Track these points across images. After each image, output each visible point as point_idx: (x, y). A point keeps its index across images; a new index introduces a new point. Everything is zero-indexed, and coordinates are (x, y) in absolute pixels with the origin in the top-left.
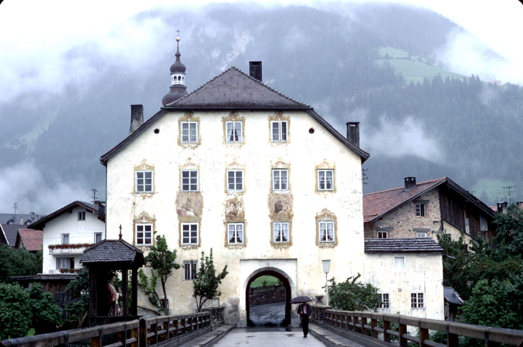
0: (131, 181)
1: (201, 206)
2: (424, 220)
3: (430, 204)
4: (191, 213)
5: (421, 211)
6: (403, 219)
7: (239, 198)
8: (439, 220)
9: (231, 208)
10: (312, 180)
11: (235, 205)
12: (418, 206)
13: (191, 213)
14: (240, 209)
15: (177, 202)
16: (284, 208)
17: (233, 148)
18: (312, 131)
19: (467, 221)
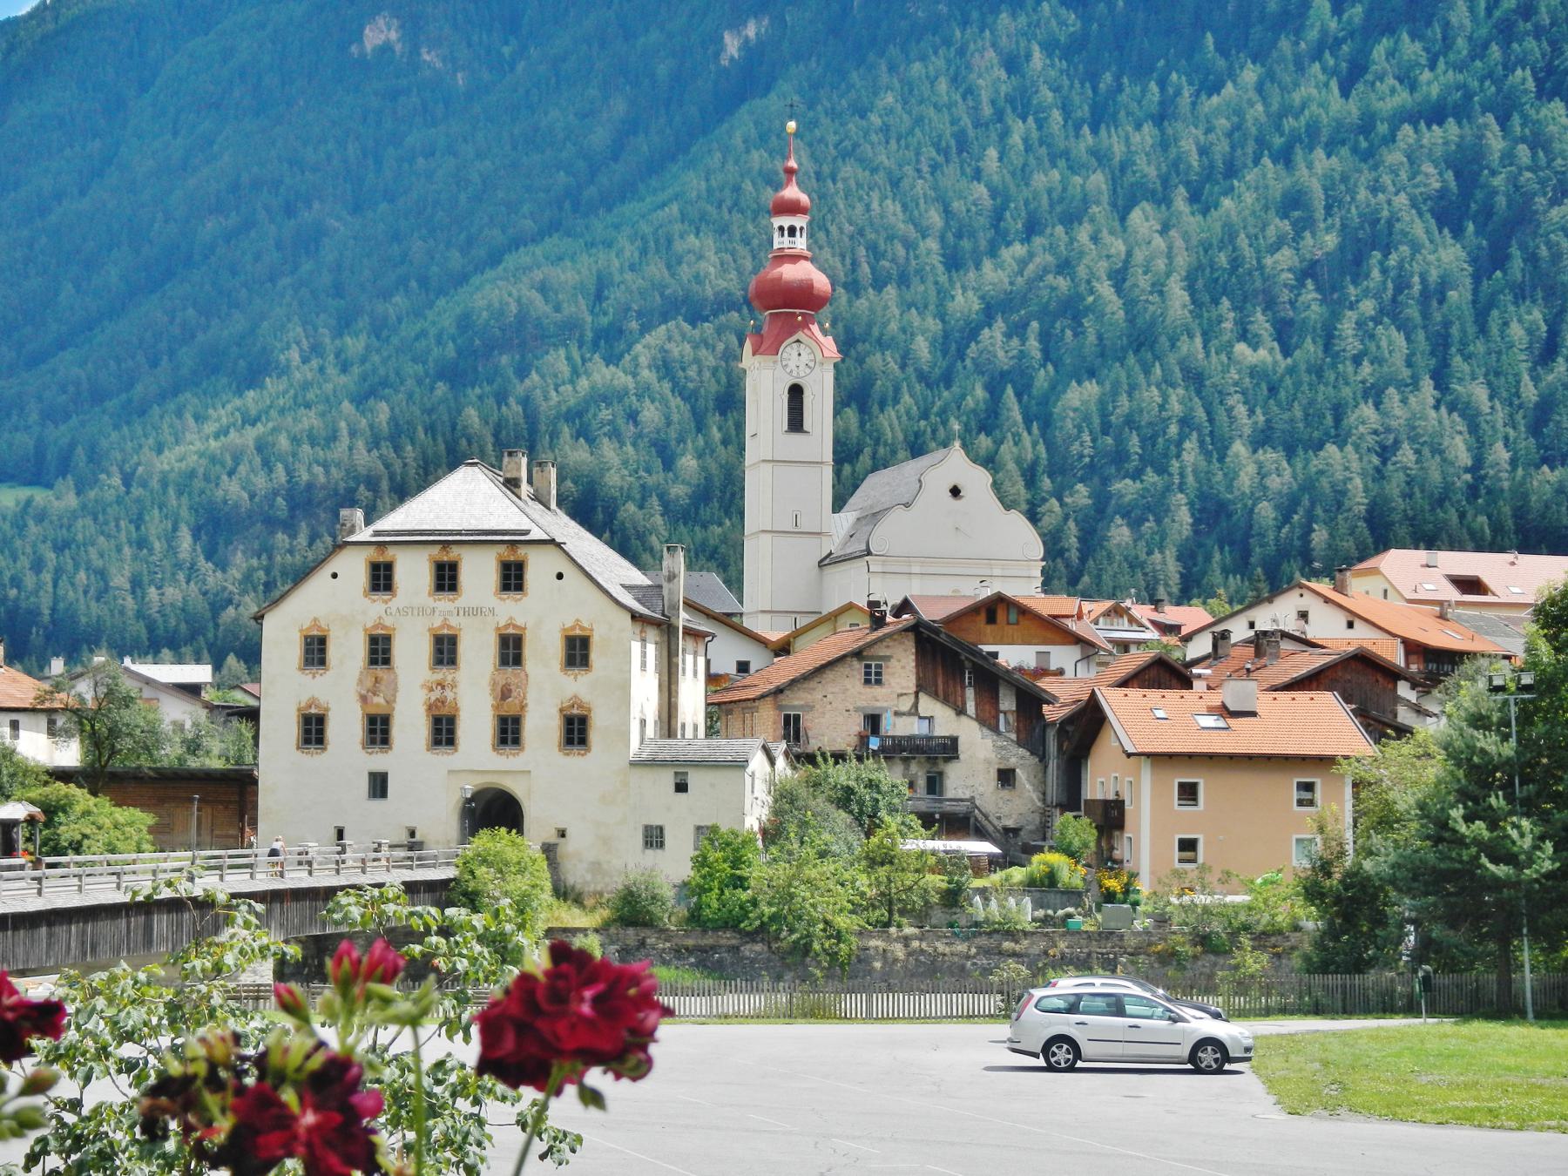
0: (296, 652)
1: (396, 690)
2: (877, 691)
3: (893, 662)
4: (379, 700)
5: (873, 678)
6: (836, 690)
7: (449, 678)
8: (913, 689)
9: (437, 694)
10: (557, 650)
11: (443, 687)
12: (868, 666)
13: (379, 700)
14: (449, 694)
15: (360, 681)
16: (514, 694)
17: (445, 603)
18: (560, 576)
19: (970, 693)
